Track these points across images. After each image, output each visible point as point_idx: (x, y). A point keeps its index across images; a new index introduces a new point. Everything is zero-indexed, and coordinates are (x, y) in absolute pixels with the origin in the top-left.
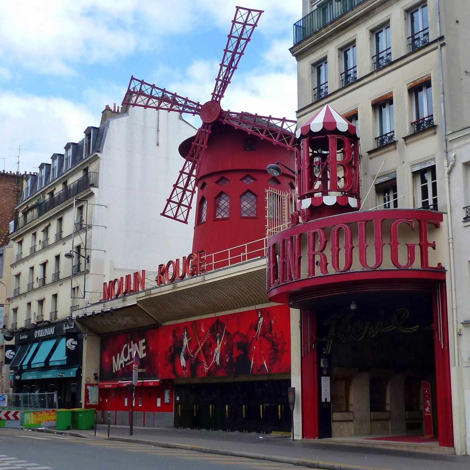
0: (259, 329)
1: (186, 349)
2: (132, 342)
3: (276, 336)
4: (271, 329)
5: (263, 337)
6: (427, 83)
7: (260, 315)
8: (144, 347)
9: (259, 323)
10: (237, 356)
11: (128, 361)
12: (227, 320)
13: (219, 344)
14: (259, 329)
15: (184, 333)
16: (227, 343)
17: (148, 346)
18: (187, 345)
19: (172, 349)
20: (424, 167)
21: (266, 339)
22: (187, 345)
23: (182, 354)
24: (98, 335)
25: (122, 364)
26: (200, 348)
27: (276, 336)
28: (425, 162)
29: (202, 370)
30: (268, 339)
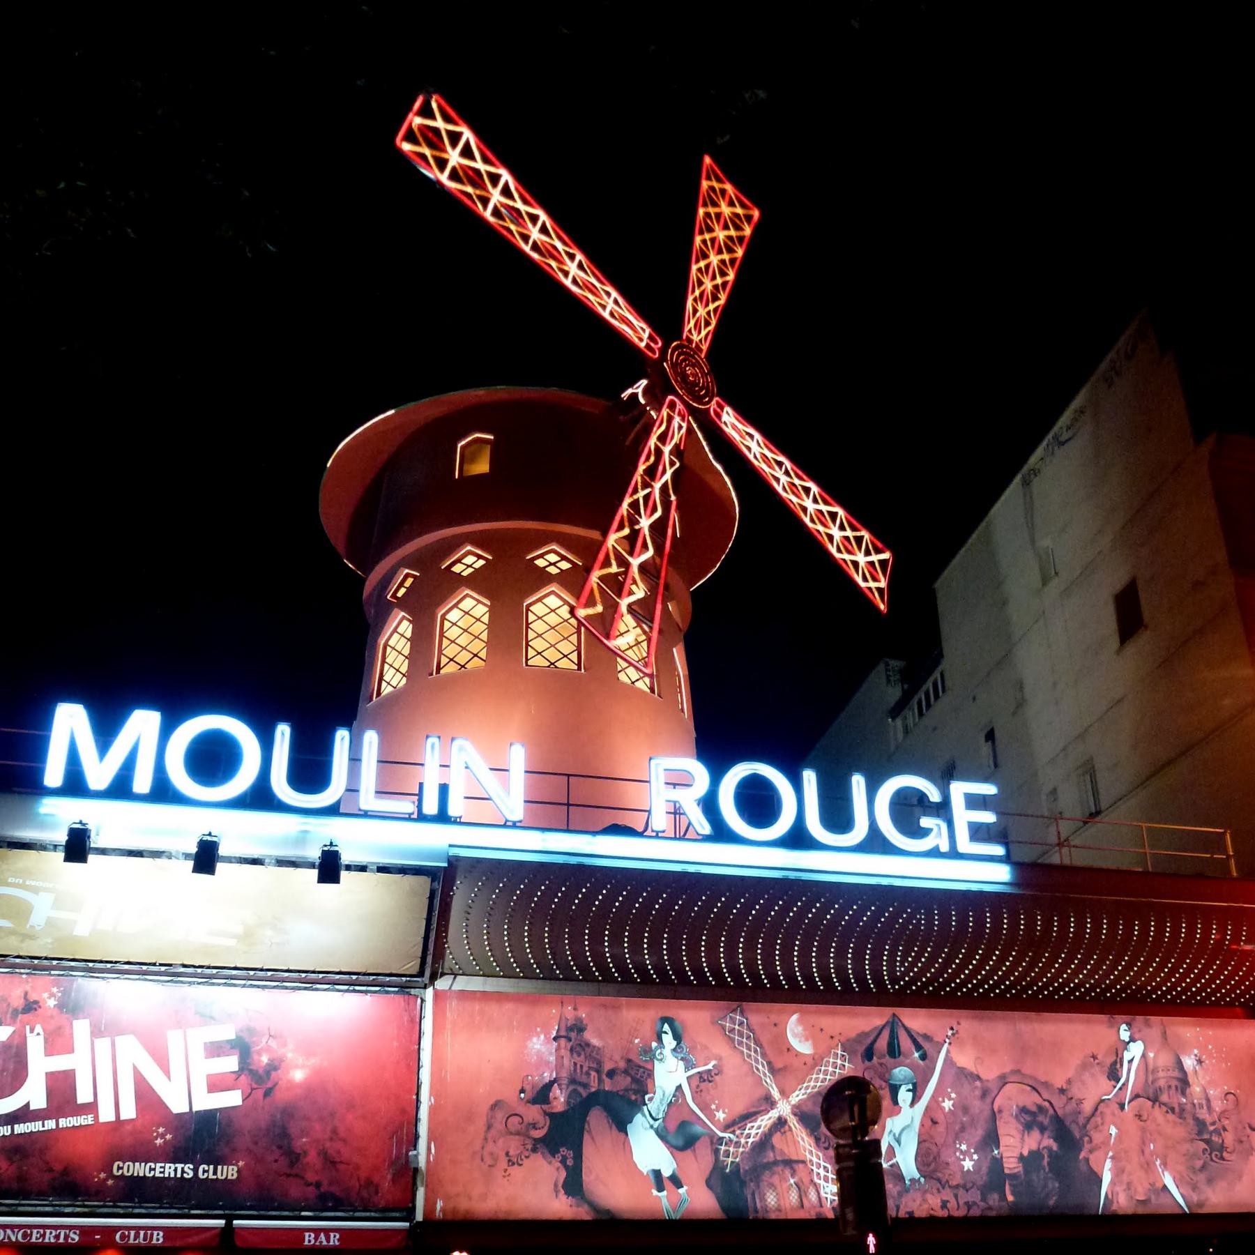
0: (1130, 1075)
3: (1209, 1107)
4: (1184, 1082)
5: (1150, 1103)
7: (1125, 1035)
8: (231, 1063)
9: (1127, 1056)
10: (1026, 1153)
12: (952, 1029)
13: (912, 1104)
15: (660, 1040)
16: (962, 1107)
17: (265, 1059)
18: (679, 1088)
19: (559, 1098)
21: (1164, 1109)
22: (679, 1088)
23: (639, 1120)
26: (783, 1109)
29: (802, 1193)
30: (1173, 1110)
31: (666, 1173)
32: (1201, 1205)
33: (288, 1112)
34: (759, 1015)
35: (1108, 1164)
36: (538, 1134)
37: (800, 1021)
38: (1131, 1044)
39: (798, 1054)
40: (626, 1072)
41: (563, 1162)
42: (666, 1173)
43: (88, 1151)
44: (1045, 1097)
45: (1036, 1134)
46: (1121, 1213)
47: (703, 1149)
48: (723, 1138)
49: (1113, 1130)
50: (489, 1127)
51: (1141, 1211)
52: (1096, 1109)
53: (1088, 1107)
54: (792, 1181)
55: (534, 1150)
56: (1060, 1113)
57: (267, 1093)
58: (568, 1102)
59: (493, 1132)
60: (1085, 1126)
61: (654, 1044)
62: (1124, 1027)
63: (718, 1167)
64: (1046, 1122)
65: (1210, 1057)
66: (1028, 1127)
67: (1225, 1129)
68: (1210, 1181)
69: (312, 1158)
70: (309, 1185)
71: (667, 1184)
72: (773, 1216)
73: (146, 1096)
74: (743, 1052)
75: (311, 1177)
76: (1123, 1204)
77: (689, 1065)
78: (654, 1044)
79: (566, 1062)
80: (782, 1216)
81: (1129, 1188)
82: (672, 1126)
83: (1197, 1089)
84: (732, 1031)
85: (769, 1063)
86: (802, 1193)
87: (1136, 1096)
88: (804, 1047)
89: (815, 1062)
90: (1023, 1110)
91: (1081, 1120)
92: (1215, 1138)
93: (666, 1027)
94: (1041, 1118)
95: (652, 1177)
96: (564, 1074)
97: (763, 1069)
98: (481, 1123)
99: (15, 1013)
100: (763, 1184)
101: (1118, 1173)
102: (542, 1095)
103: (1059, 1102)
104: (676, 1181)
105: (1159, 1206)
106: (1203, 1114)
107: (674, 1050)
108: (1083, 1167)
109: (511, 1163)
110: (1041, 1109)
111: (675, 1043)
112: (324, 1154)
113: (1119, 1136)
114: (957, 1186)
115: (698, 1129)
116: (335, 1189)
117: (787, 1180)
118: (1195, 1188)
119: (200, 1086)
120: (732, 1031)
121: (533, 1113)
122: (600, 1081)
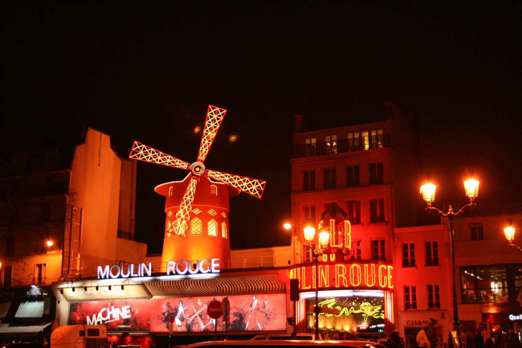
0: (254, 306)
1: (182, 314)
2: (113, 307)
3: (269, 311)
4: (264, 307)
6: (382, 201)
8: (129, 311)
9: (254, 302)
10: (234, 320)
11: (108, 320)
14: (254, 306)
17: (133, 310)
18: (182, 312)
19: (166, 314)
20: (378, 239)
21: (260, 312)
22: (182, 312)
24: (68, 300)
25: (99, 323)
26: (197, 314)
27: (269, 311)
28: (380, 238)
29: (198, 327)
30: (261, 312)
31: (180, 325)
32: (264, 329)
33: (136, 318)
34: (194, 299)
35: (248, 322)
36: (164, 319)
37: (200, 300)
38: (256, 300)
39: (199, 305)
40: (175, 310)
41: (167, 323)
42: (180, 325)
43: (115, 324)
44: (238, 310)
45: (236, 317)
46: (249, 330)
47: (185, 321)
48: (187, 320)
49: (250, 316)
50: (157, 319)
51: (253, 330)
52: (247, 312)
53: (246, 312)
54: (197, 326)
55: (163, 322)
56: (241, 313)
57: (134, 315)
58: (167, 315)
59: (158, 319)
60: (245, 315)
61: (179, 305)
62: (254, 297)
63: (187, 324)
64: (238, 315)
65: (270, 301)
66: (235, 316)
67: (271, 315)
68: (266, 325)
69: (139, 324)
70: (138, 327)
71: (180, 326)
72: (194, 331)
73: (120, 317)
74: (191, 305)
75: (139, 327)
76: (250, 329)
77: (184, 308)
78: (179, 305)
79: (167, 309)
80: (195, 331)
81: (251, 326)
82: (181, 318)
83: (267, 308)
84: (190, 302)
85: (195, 307)
86: (198, 327)
87: (255, 310)
88: (200, 304)
89: (202, 306)
90: (234, 313)
91: (244, 314)
92: (269, 317)
93: (181, 302)
94: (237, 314)
95: (178, 326)
96: (167, 310)
97: (194, 308)
98: (156, 318)
99: (106, 306)
100: (193, 326)
101: (249, 324)
102: (164, 314)
103: (241, 311)
104: (181, 326)
105: (256, 329)
106: (267, 313)
107: (182, 306)
108: (244, 322)
109: (160, 324)
110: (237, 313)
111: (182, 305)
112: (140, 323)
113: (251, 317)
114: (222, 326)
115: (184, 318)
116: (142, 328)
117: (196, 325)
118: (263, 326)
119: (126, 314)
120: (190, 302)
121: (163, 317)
122: (172, 311)
